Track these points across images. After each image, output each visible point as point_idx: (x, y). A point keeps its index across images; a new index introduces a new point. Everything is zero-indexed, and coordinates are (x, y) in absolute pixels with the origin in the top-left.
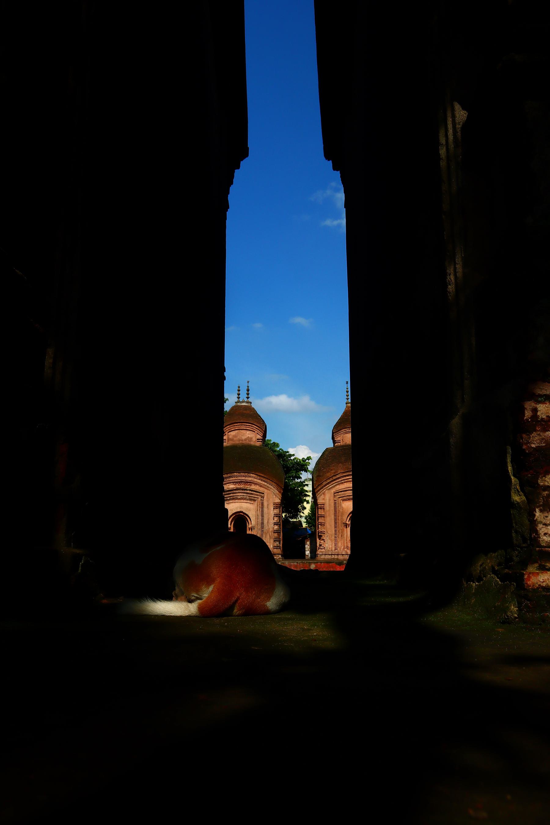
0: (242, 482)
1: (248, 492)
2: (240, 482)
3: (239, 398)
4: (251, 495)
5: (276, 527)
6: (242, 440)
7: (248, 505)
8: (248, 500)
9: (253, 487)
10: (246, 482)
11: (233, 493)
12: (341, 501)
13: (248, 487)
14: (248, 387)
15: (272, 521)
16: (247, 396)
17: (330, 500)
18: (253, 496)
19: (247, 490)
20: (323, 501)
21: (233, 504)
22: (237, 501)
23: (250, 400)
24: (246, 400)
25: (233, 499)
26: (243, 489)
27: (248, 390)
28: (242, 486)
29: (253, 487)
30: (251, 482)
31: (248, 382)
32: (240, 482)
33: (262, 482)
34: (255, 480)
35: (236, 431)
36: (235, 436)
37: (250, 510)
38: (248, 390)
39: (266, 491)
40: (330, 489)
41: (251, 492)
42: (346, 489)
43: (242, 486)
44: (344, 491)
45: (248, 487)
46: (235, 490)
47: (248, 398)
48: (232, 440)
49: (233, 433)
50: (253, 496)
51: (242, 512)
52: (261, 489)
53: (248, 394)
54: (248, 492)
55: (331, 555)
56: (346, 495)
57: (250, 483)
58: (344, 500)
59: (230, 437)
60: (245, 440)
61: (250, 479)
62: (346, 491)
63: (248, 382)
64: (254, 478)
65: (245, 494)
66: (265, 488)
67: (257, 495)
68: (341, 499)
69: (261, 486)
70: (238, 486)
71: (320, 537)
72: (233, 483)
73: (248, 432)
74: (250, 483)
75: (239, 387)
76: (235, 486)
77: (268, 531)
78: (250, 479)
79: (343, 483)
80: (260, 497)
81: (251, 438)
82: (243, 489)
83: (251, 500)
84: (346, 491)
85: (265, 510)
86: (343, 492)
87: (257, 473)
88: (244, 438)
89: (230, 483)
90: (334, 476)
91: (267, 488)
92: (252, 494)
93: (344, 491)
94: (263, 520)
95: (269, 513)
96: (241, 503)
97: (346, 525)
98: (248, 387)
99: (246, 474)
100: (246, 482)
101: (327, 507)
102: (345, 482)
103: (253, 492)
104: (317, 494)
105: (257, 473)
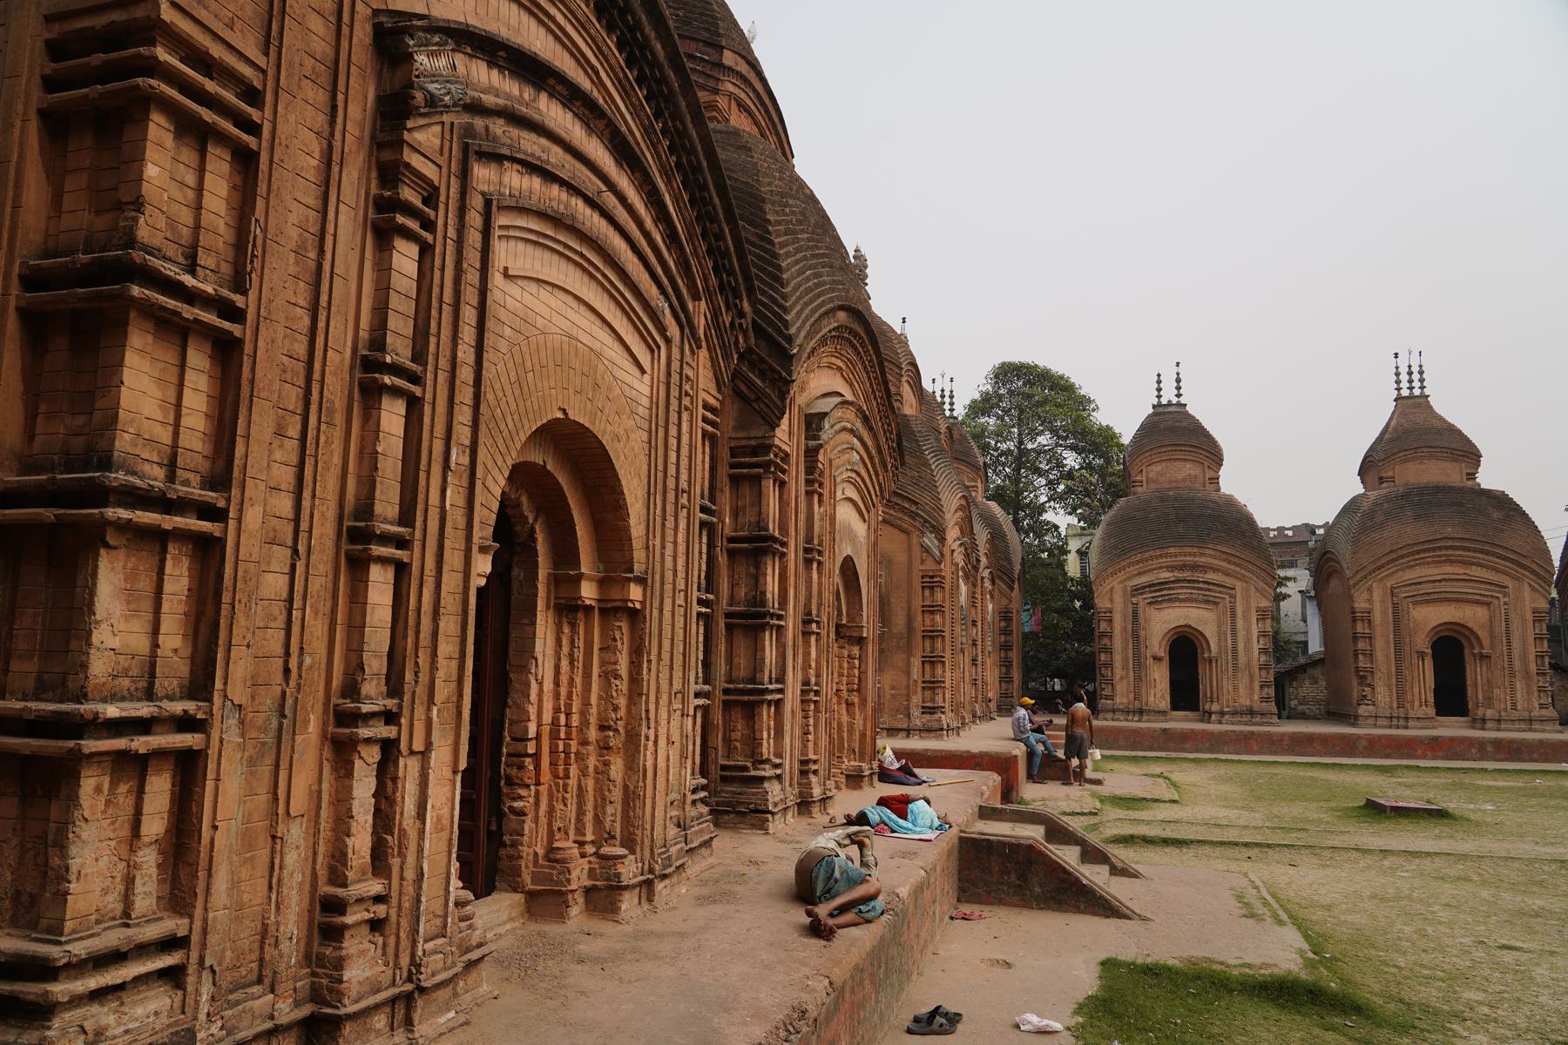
0: (1185, 566)
1: (1201, 585)
2: (1183, 567)
3: (1159, 397)
4: (1207, 593)
5: (1263, 658)
6: (1177, 482)
7: (1201, 612)
8: (1200, 602)
9: (1210, 576)
10: (1195, 567)
11: (1169, 589)
12: (1410, 605)
13: (1201, 577)
14: (1178, 374)
15: (1256, 647)
16: (1176, 392)
17: (1383, 602)
18: (1213, 594)
19: (1199, 582)
20: (1367, 605)
21: (1171, 610)
22: (1177, 604)
23: (1183, 400)
24: (1175, 400)
25: (1170, 600)
26: (1189, 581)
27: (1178, 380)
28: (1186, 575)
29: (1210, 576)
30: (1204, 567)
31: (1178, 364)
32: (1183, 567)
33: (1230, 566)
34: (1216, 562)
35: (1164, 464)
36: (1163, 475)
37: (1206, 624)
38: (1178, 380)
39: (1238, 584)
40: (1382, 579)
41: (1206, 586)
42: (1419, 580)
43: (1186, 575)
44: (1415, 584)
45: (1201, 577)
46: (1173, 582)
47: (1179, 395)
48: (1155, 481)
49: (1156, 468)
50: (1213, 594)
51: (1189, 626)
52: (1229, 581)
53: (1178, 388)
54: (1201, 585)
55: (1391, 718)
56: (1422, 592)
57: (1204, 568)
58: (1416, 603)
59: (1152, 475)
60: (1183, 480)
61: (1203, 559)
62: (1420, 583)
63: (1178, 364)
64: (1214, 557)
65: (1195, 591)
66: (1237, 578)
67: (1220, 592)
68: (1409, 600)
69: (1227, 574)
70: (1178, 574)
71: (1362, 680)
72: (1167, 567)
73: (1188, 465)
74: (1204, 568)
75: (1159, 375)
76: (1171, 575)
77: (1248, 665)
78: (1203, 559)
79: (1411, 567)
80: (1227, 597)
81: (1196, 477)
82: (1189, 581)
83: (1207, 602)
84: (1420, 583)
85: (1240, 624)
86: (1413, 587)
87: (1219, 548)
88: (1179, 477)
89: (1161, 568)
90: (1392, 551)
91: (1242, 579)
92: (1209, 590)
93: (1415, 584)
94: (1235, 642)
95: (1248, 630)
96: (1186, 609)
97: (1422, 655)
98: (1178, 374)
99: (1195, 550)
100: (1195, 567)
101: (1377, 617)
102: (1417, 565)
103: (1210, 587)
104: (1353, 591)
105: (1219, 548)
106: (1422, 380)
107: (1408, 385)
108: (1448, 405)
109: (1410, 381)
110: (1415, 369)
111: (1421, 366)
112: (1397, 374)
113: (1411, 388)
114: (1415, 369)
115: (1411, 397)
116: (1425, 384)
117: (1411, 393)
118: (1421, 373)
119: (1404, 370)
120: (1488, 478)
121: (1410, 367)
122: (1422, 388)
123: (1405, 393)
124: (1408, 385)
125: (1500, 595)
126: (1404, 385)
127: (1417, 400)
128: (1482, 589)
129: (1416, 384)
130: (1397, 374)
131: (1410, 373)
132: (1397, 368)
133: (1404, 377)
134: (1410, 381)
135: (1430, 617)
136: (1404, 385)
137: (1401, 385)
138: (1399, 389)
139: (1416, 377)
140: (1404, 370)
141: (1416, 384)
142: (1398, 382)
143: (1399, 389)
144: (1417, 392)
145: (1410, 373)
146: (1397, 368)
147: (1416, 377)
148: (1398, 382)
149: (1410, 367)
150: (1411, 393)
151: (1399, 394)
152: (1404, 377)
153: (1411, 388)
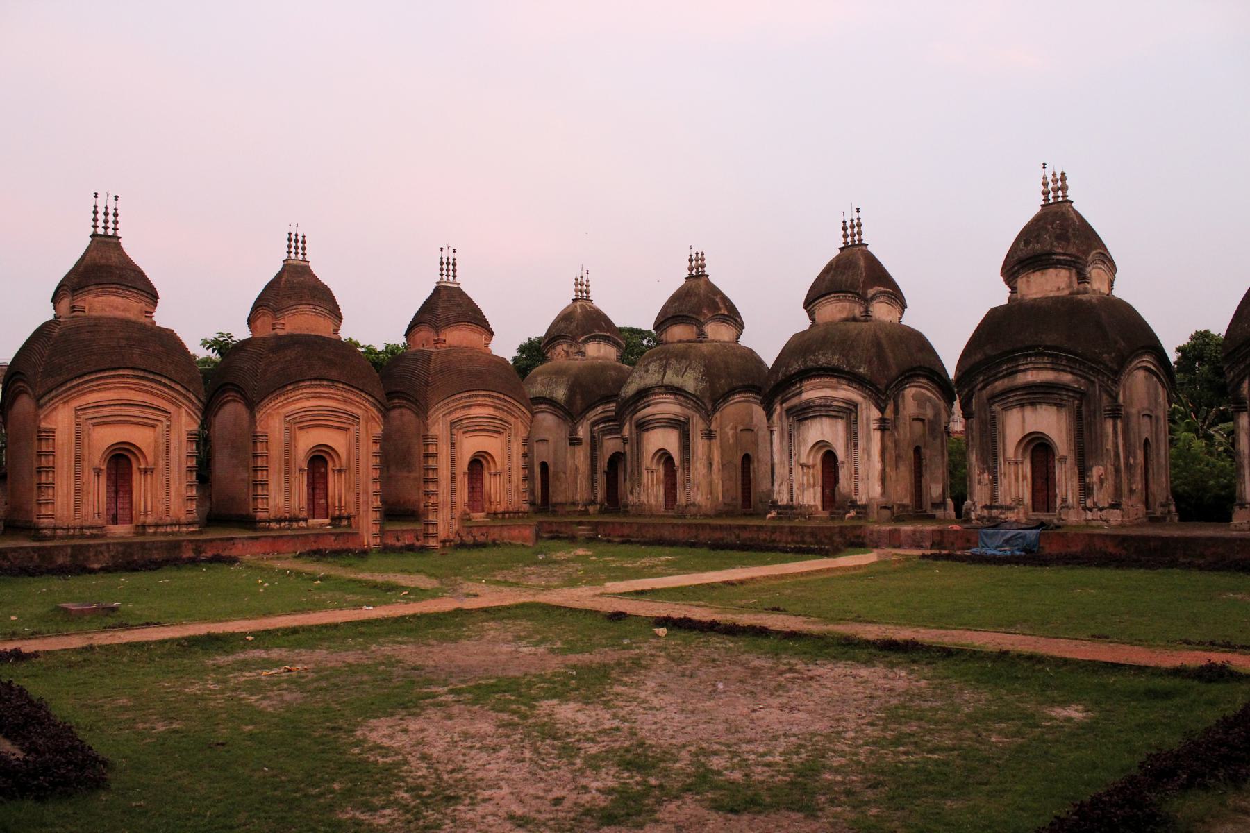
12: (91, 427)
58: (94, 425)
68: (90, 422)
93: (97, 407)
97: (98, 472)
106: (116, 223)
107: (103, 225)
108: (135, 248)
109: (106, 221)
110: (111, 211)
111: (116, 209)
112: (95, 213)
113: (106, 228)
114: (111, 211)
115: (106, 235)
116: (118, 226)
117: (106, 232)
118: (116, 215)
119: (101, 210)
120: (163, 318)
121: (107, 208)
122: (115, 229)
123: (100, 231)
124: (103, 225)
125: (164, 419)
126: (101, 223)
127: (110, 240)
128: (152, 414)
129: (111, 225)
130: (95, 213)
131: (106, 214)
132: (95, 207)
133: (101, 217)
134: (106, 221)
135: (107, 437)
136: (101, 223)
137: (98, 224)
138: (95, 227)
139: (111, 218)
140: (101, 210)
141: (111, 225)
142: (95, 220)
143: (95, 227)
144: (110, 232)
145: (106, 214)
146: (95, 207)
147: (111, 218)
148: (95, 220)
149: (107, 208)
150: (106, 232)
151: (95, 232)
152: (101, 217)
153: (106, 228)
